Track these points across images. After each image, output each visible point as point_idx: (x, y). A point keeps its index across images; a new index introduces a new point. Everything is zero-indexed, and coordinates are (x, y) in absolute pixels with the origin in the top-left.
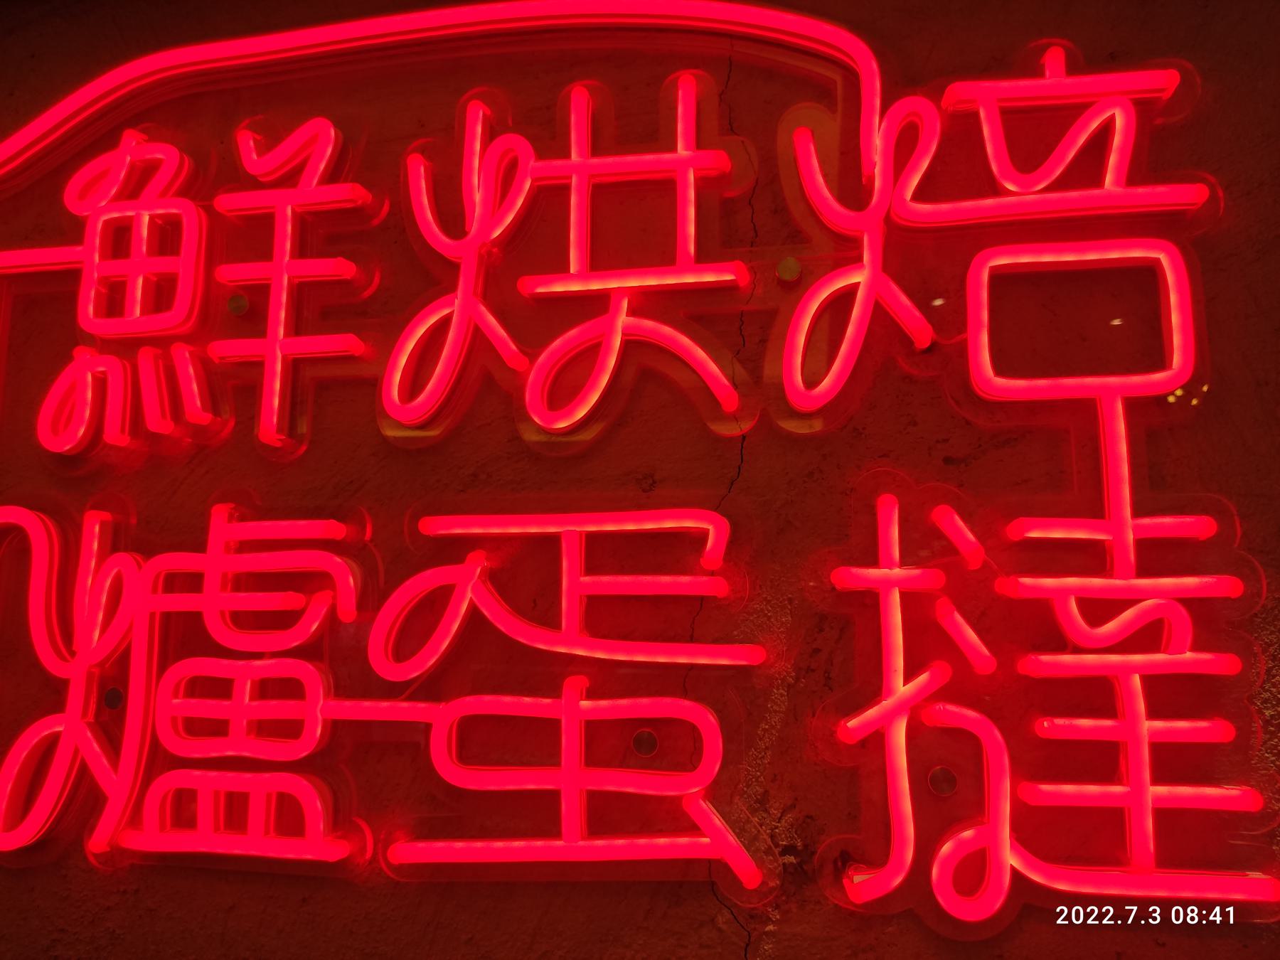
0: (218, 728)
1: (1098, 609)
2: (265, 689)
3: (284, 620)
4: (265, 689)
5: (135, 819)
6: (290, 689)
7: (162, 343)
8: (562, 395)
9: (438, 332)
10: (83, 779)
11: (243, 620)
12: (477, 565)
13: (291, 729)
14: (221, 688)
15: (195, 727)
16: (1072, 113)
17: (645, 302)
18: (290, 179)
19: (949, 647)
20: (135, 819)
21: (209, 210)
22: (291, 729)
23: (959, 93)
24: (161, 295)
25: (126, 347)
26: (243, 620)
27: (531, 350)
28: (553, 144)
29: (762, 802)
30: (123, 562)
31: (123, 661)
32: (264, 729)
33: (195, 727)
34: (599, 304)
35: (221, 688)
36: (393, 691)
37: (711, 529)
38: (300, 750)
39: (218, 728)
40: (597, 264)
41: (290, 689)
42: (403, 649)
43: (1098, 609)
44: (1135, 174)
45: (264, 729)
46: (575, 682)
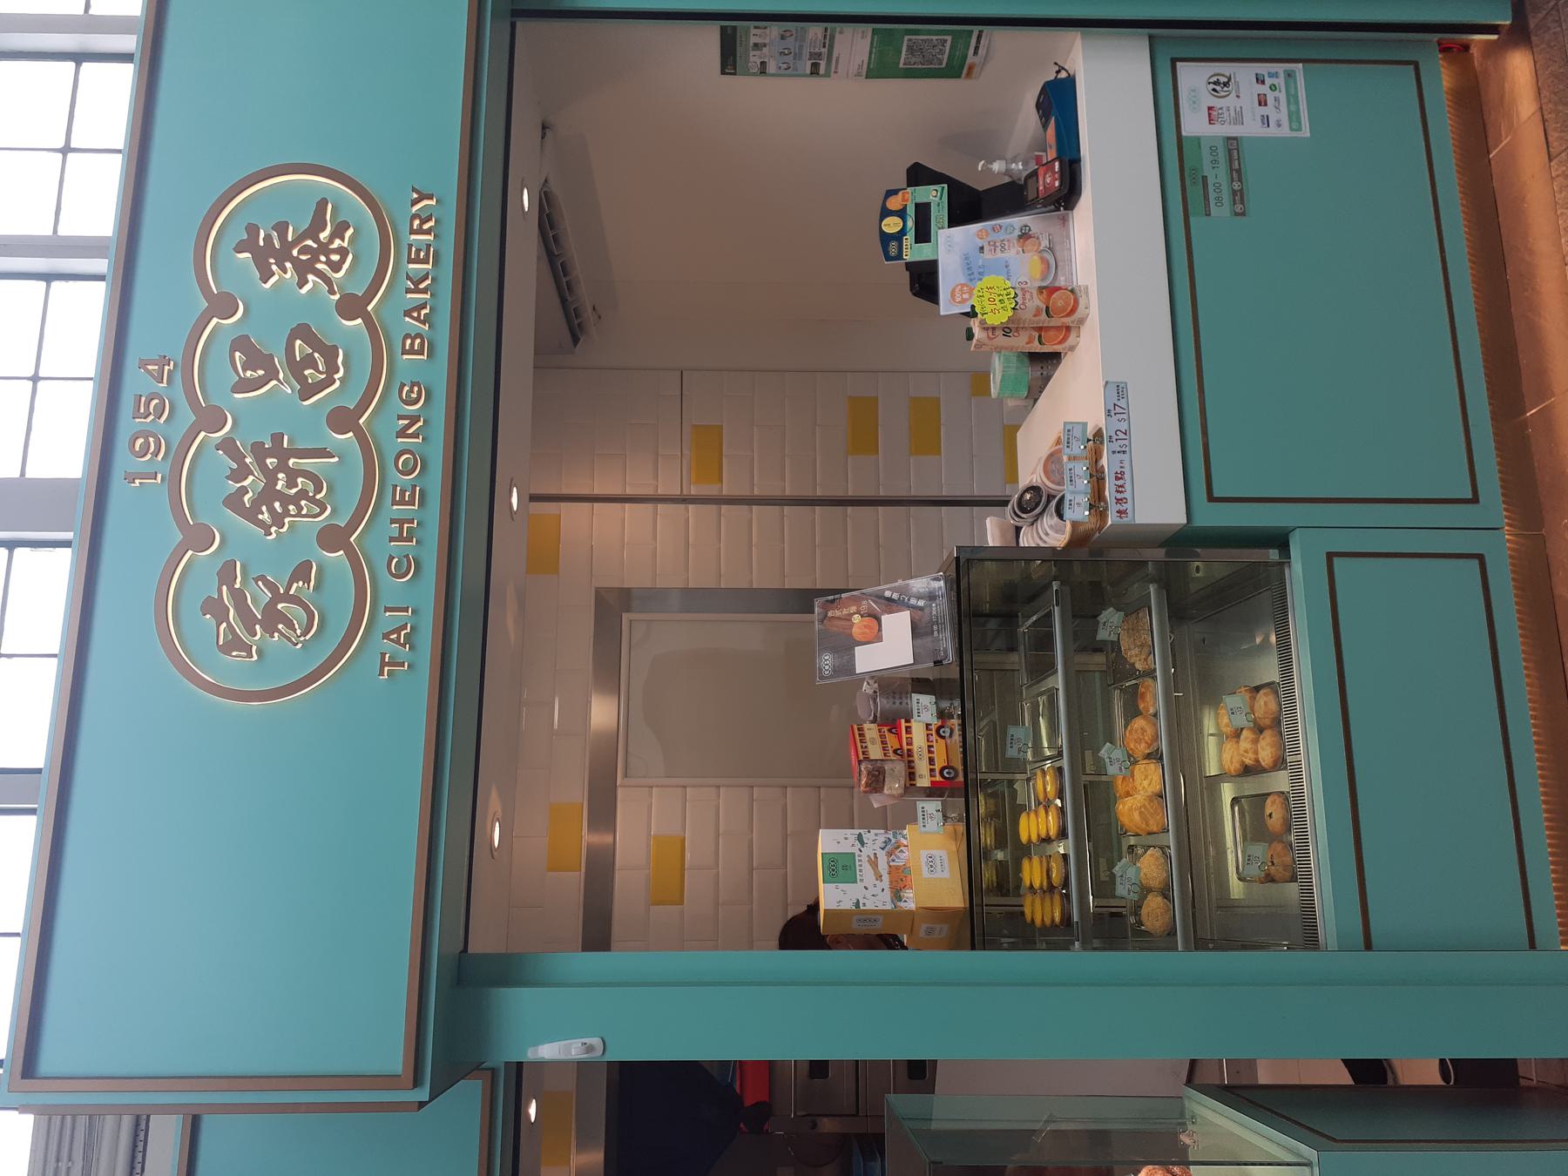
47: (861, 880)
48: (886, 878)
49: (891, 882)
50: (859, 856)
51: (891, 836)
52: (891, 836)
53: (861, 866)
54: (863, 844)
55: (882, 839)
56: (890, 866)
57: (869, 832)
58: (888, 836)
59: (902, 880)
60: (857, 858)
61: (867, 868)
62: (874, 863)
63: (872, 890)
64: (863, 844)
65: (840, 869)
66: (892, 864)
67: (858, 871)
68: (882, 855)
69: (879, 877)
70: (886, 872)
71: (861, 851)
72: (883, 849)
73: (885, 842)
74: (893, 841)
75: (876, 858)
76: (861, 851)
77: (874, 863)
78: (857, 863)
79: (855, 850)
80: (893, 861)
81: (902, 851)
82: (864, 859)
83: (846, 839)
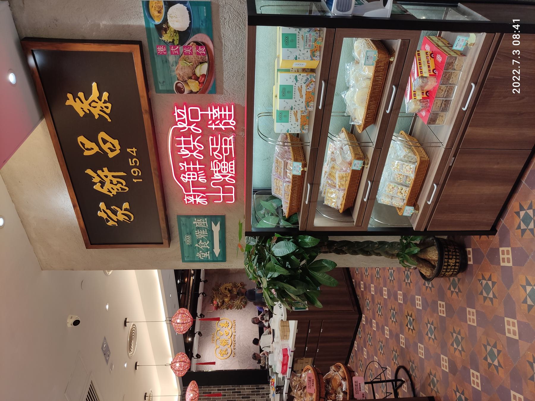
0: (226, 169)
1: (215, 115)
2: (223, 166)
3: (218, 165)
4: (223, 166)
5: (233, 174)
6: (223, 164)
7: (198, 174)
8: (201, 147)
9: (197, 155)
10: (230, 177)
11: (218, 167)
12: (214, 152)
13: (226, 164)
14: (223, 169)
15: (226, 170)
16: (178, 113)
17: (194, 142)
18: (184, 166)
19: (219, 123)
20: (233, 174)
21: (187, 172)
22: (226, 164)
23: (177, 121)
24: (193, 175)
25: (198, 177)
26: (218, 167)
27: (198, 149)
28: (181, 148)
29: (229, 134)
30: (215, 176)
31: (221, 175)
32: (226, 166)
33: (226, 170)
34: (194, 145)
35: (223, 169)
36: (223, 157)
37: (211, 137)
38: (227, 163)
39: (226, 169)
40: (191, 144)
41: (223, 164)
42: (220, 157)
43: (215, 115)
44: (183, 109)
45: (226, 166)
46: (222, 146)
47: (294, 98)
48: (304, 97)
49: (306, 98)
50: (295, 87)
51: (309, 77)
52: (309, 77)
53: (295, 91)
54: (297, 80)
55: (305, 78)
56: (306, 92)
57: (300, 75)
58: (307, 77)
59: (310, 98)
60: (294, 87)
61: (297, 93)
62: (300, 90)
63: (294, 126)
64: (297, 80)
65: (287, 92)
66: (307, 90)
67: (293, 93)
68: (304, 86)
69: (302, 96)
70: (305, 94)
71: (296, 84)
72: (305, 83)
73: (306, 80)
74: (309, 79)
75: (301, 87)
76: (296, 84)
77: (300, 90)
78: (294, 90)
79: (293, 84)
80: (308, 89)
81: (312, 84)
82: (297, 88)
83: (290, 78)
